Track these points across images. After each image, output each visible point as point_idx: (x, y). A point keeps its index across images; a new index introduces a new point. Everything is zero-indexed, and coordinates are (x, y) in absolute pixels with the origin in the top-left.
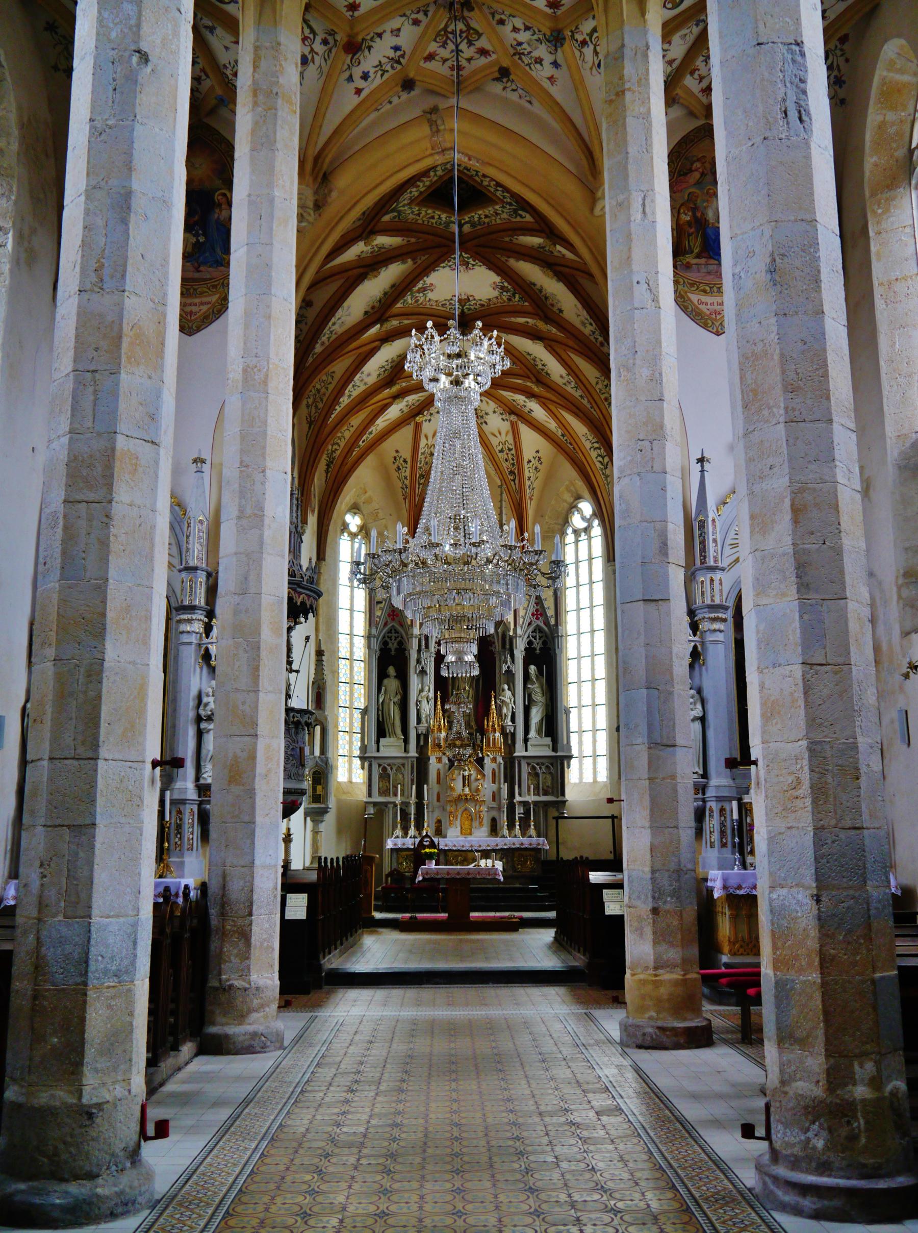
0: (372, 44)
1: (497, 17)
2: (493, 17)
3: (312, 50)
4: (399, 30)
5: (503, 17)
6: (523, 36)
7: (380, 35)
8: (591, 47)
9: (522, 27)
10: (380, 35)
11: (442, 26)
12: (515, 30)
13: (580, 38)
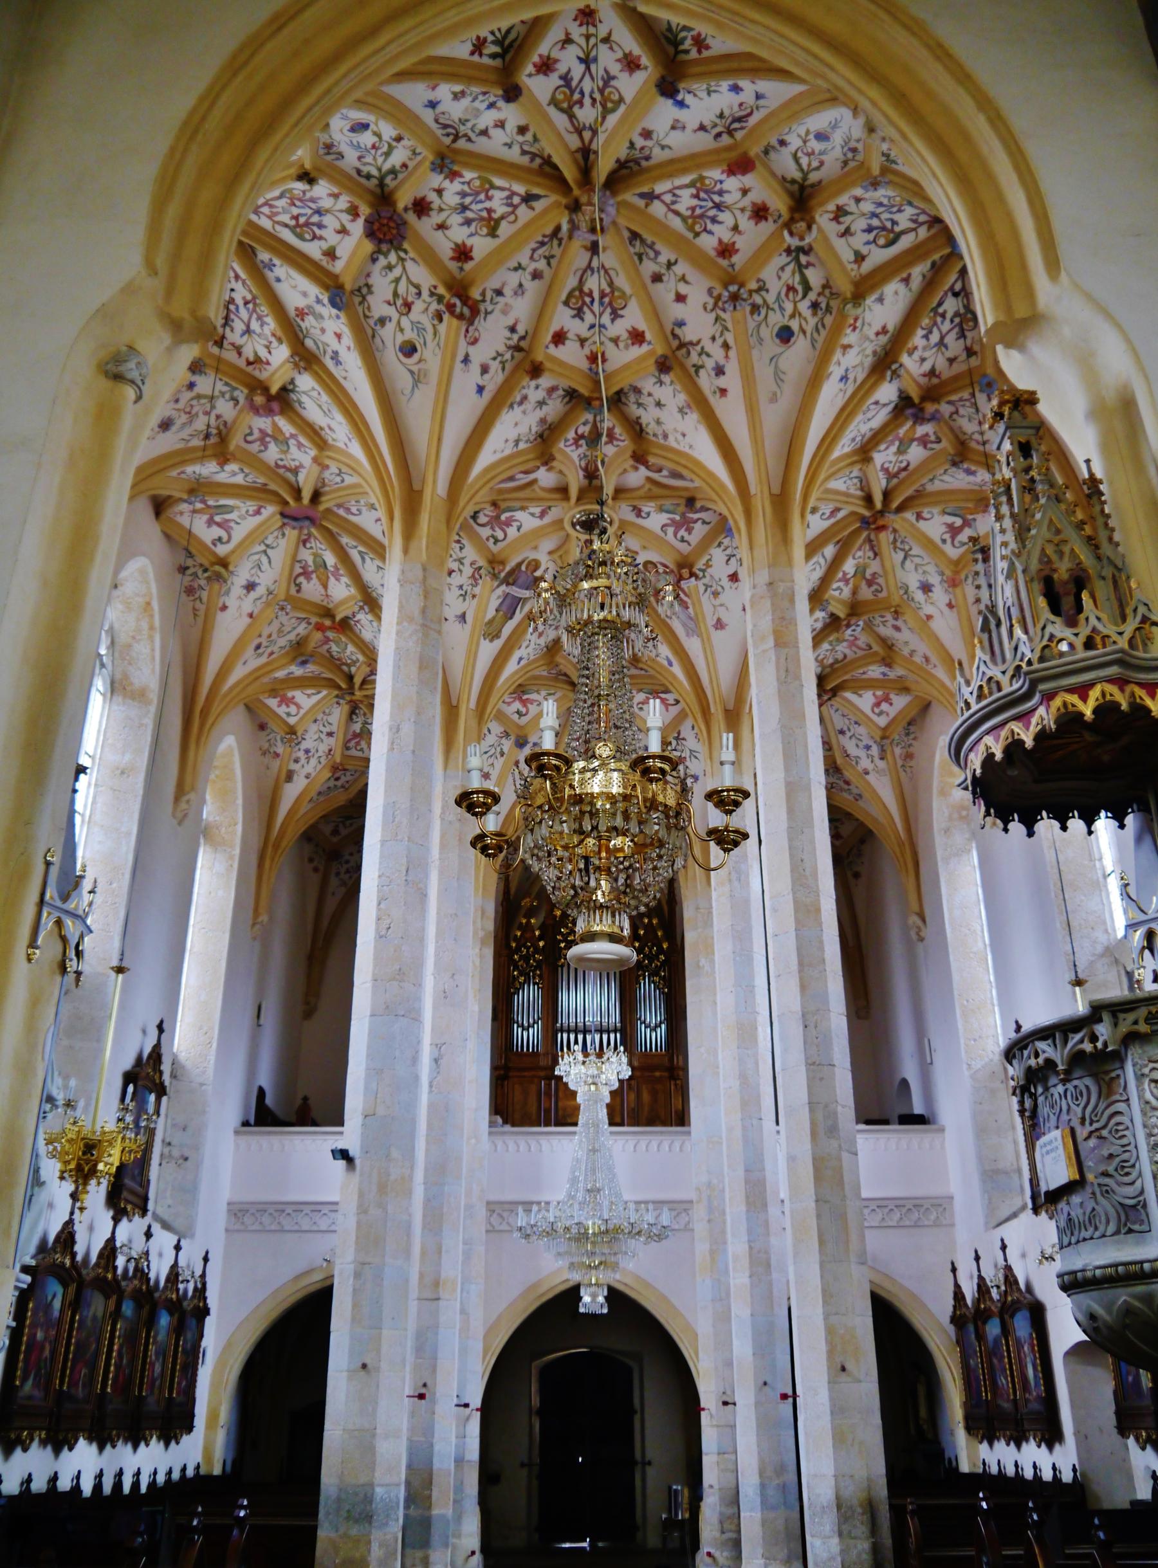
0: (718, 121)
1: (529, 136)
2: (535, 136)
3: (805, 142)
4: (673, 128)
5: (520, 138)
6: (487, 119)
7: (702, 128)
8: (386, 137)
9: (492, 132)
10: (702, 128)
11: (612, 119)
12: (501, 124)
13: (405, 142)
